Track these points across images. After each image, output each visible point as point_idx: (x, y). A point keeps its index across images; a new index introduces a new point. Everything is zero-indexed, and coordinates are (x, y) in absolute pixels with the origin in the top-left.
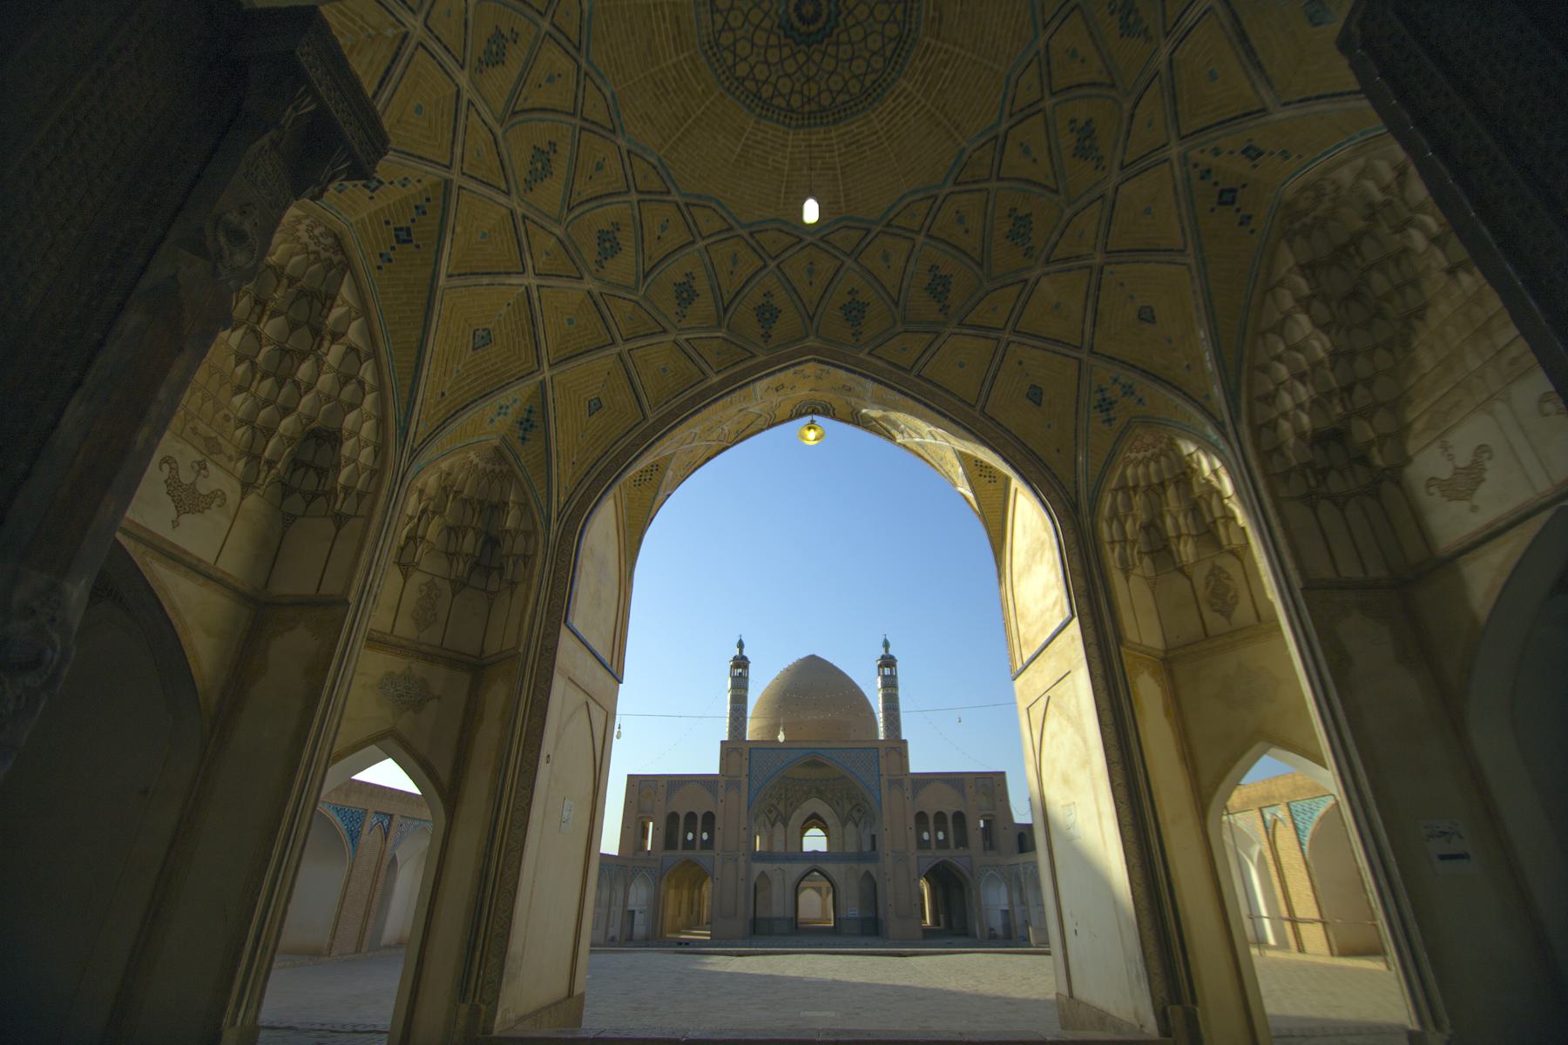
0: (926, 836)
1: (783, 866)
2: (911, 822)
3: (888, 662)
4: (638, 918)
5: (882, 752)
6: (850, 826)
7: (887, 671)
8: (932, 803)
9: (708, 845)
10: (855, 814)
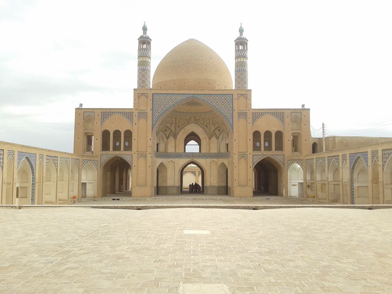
0: (258, 144)
1: (173, 160)
2: (251, 137)
3: (241, 43)
4: (88, 187)
5: (235, 97)
6: (214, 139)
7: (241, 47)
8: (262, 126)
9: (129, 148)
10: (217, 132)
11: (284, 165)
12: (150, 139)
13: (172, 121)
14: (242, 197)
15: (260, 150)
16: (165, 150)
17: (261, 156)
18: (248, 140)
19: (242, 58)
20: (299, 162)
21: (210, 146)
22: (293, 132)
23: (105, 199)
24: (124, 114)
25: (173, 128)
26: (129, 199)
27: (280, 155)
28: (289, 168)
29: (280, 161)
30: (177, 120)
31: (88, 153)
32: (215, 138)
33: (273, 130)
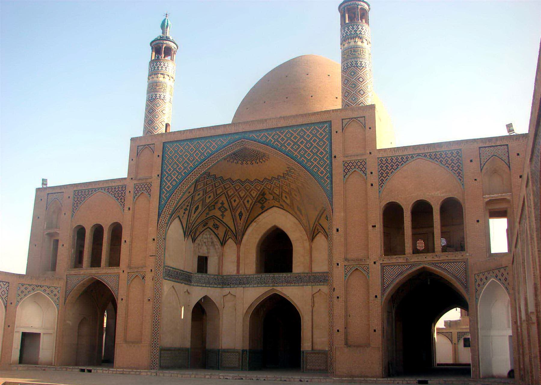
1: (233, 291)
5: (337, 126)
6: (320, 239)
9: (114, 262)
11: (466, 287)
12: (154, 240)
13: (223, 203)
14: (352, 376)
15: (403, 252)
16: (219, 270)
17: (404, 268)
18: (370, 227)
19: (352, 40)
20: (499, 276)
21: (311, 257)
22: (487, 197)
23: (67, 369)
24: (110, 190)
25: (228, 219)
26: (109, 370)
27: (455, 261)
28: (479, 295)
29: (456, 277)
30: (233, 202)
31: (50, 273)
32: (323, 237)
33: (435, 197)
